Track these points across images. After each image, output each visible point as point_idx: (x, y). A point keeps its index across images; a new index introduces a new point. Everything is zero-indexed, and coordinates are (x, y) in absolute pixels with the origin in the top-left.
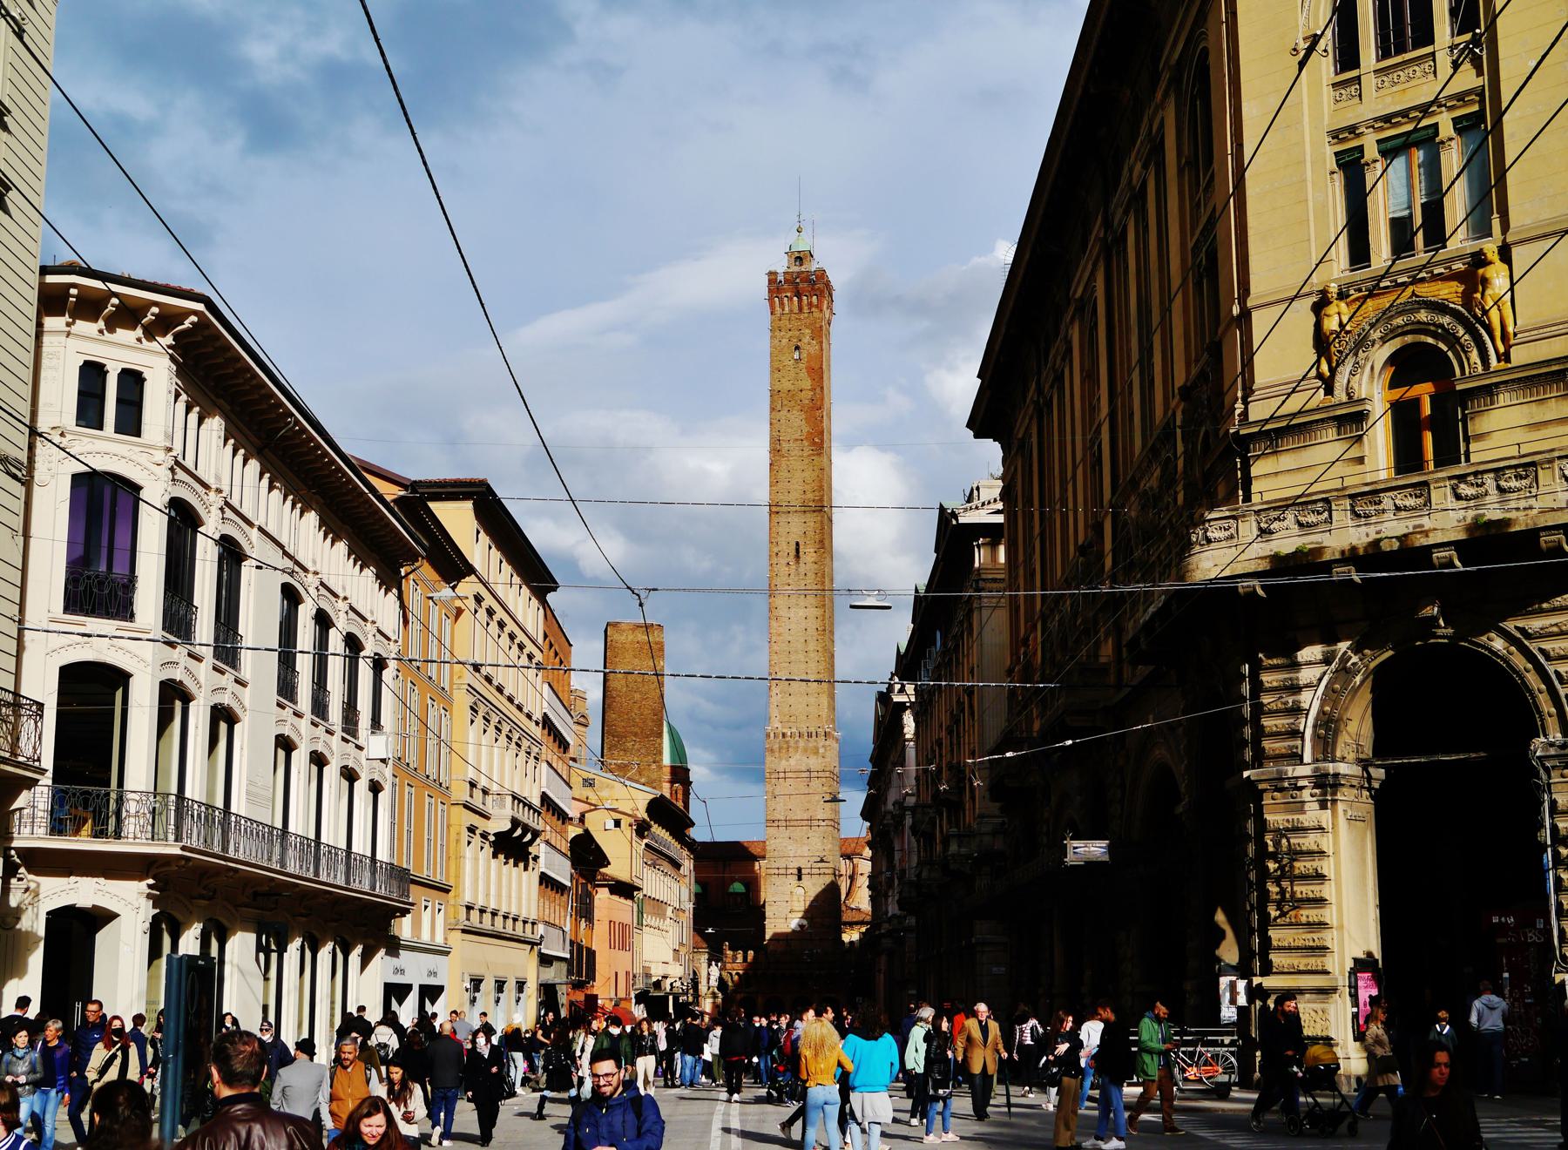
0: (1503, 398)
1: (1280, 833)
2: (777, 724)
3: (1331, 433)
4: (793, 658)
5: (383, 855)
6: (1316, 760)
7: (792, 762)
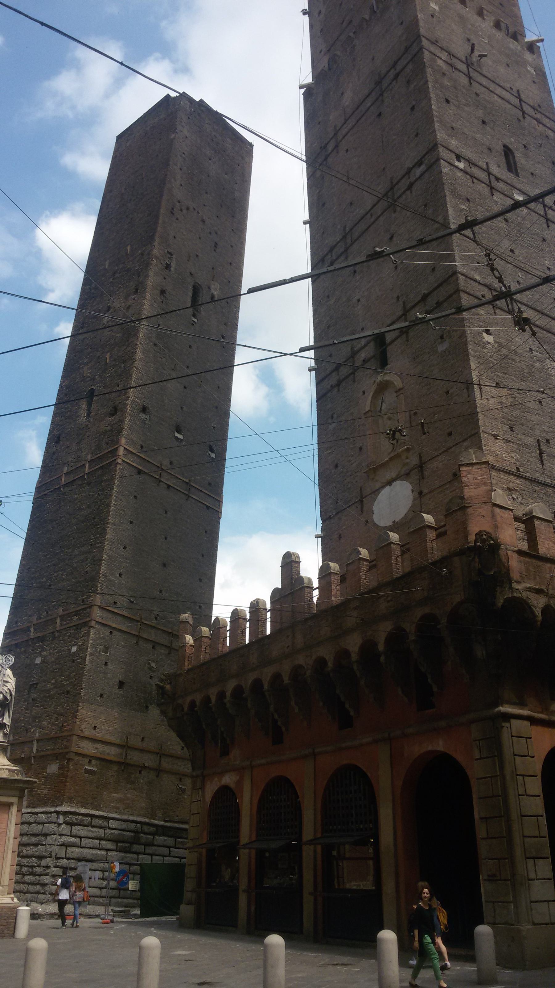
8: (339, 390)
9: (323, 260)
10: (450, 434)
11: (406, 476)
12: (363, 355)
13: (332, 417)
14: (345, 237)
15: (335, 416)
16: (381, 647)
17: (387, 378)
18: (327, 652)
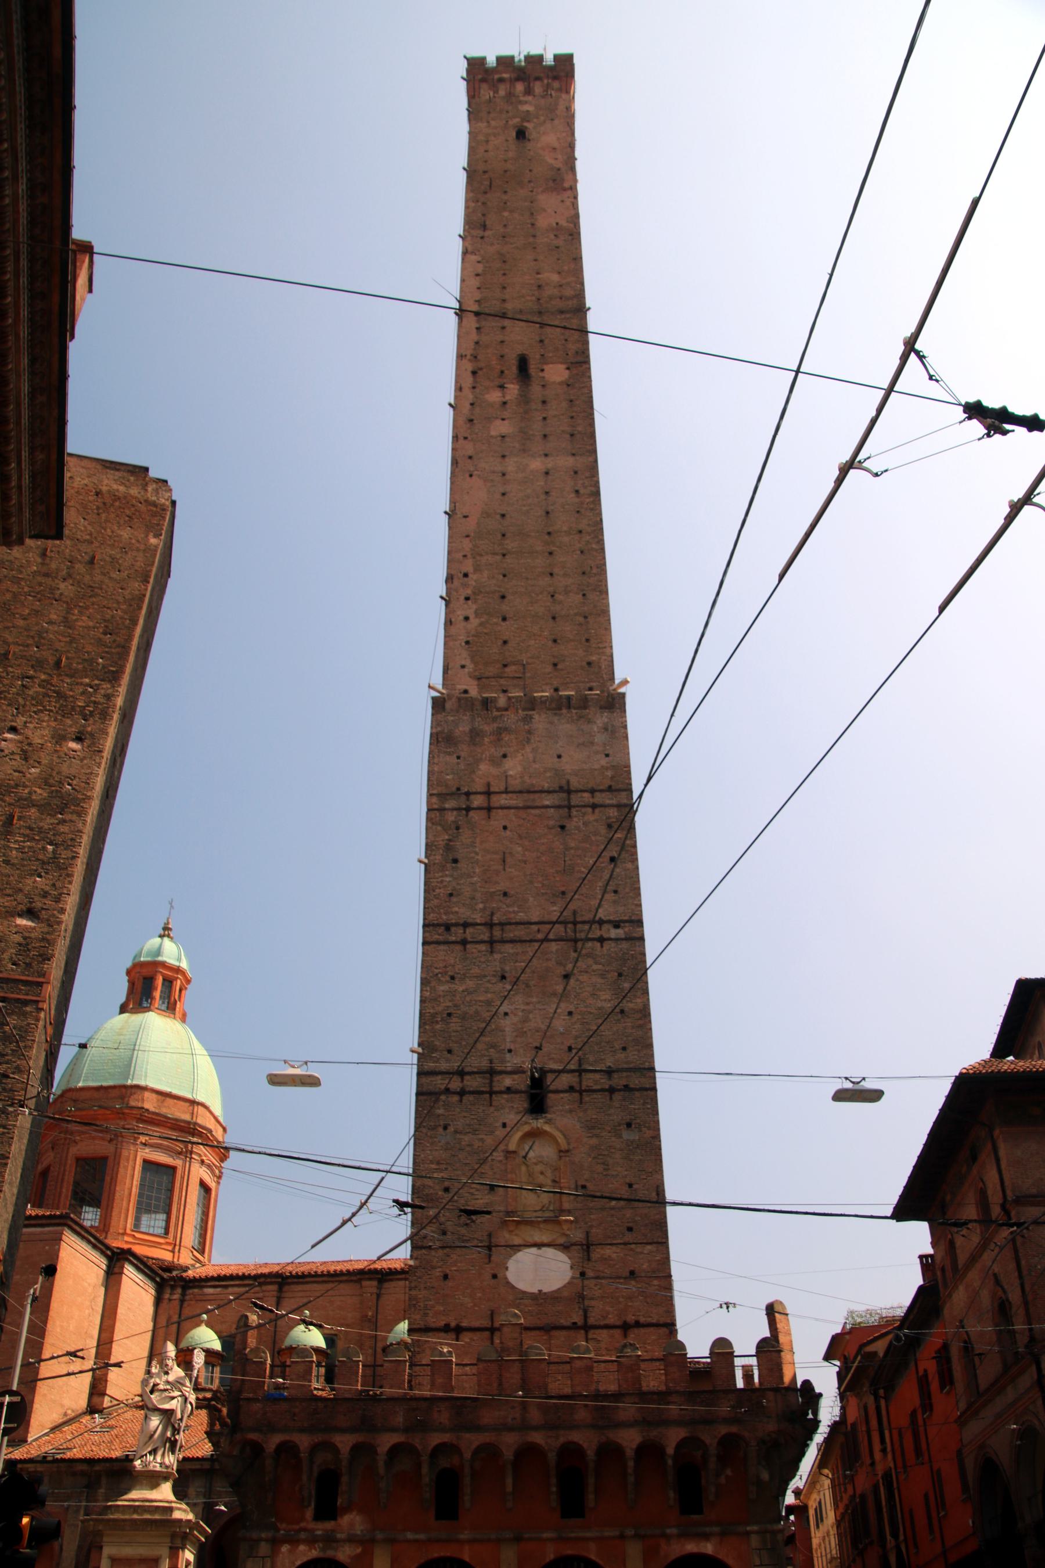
4: (511, 545)
7: (513, 767)
8: (461, 1101)
9: (448, 927)
10: (630, 1229)
11: (565, 1248)
12: (508, 1081)
13: (445, 1128)
14: (490, 925)
15: (451, 1129)
16: (670, 1451)
17: (547, 1128)
18: (587, 1440)
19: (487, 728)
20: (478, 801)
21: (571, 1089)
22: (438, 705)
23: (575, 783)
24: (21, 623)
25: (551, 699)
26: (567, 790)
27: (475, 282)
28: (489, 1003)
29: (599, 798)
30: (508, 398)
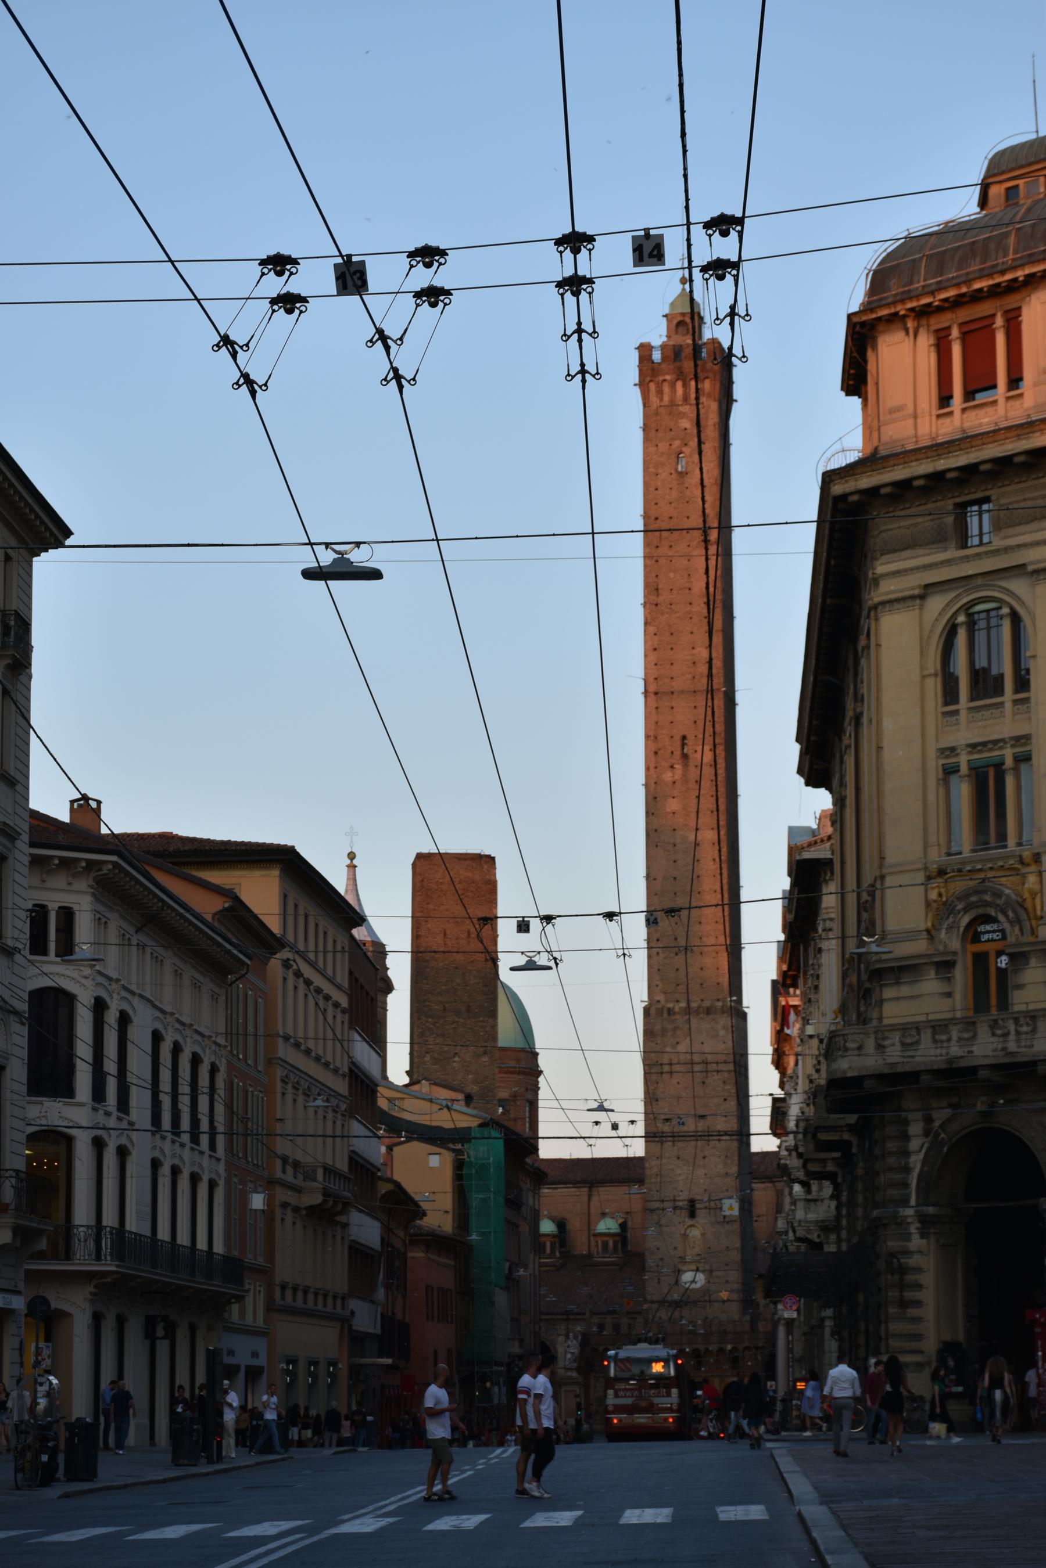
0: (1033, 962)
1: (892, 1255)
2: (660, 997)
3: (932, 973)
5: (219, 1248)
6: (917, 1205)
7: (681, 1048)
18: (702, 1348)
19: (670, 1027)
20: (666, 1068)
21: (706, 1208)
22: (647, 1011)
23: (710, 1058)
24: (444, 988)
25: (699, 1007)
26: (706, 1063)
27: (653, 657)
28: (673, 1170)
29: (721, 1067)
30: (676, 777)
